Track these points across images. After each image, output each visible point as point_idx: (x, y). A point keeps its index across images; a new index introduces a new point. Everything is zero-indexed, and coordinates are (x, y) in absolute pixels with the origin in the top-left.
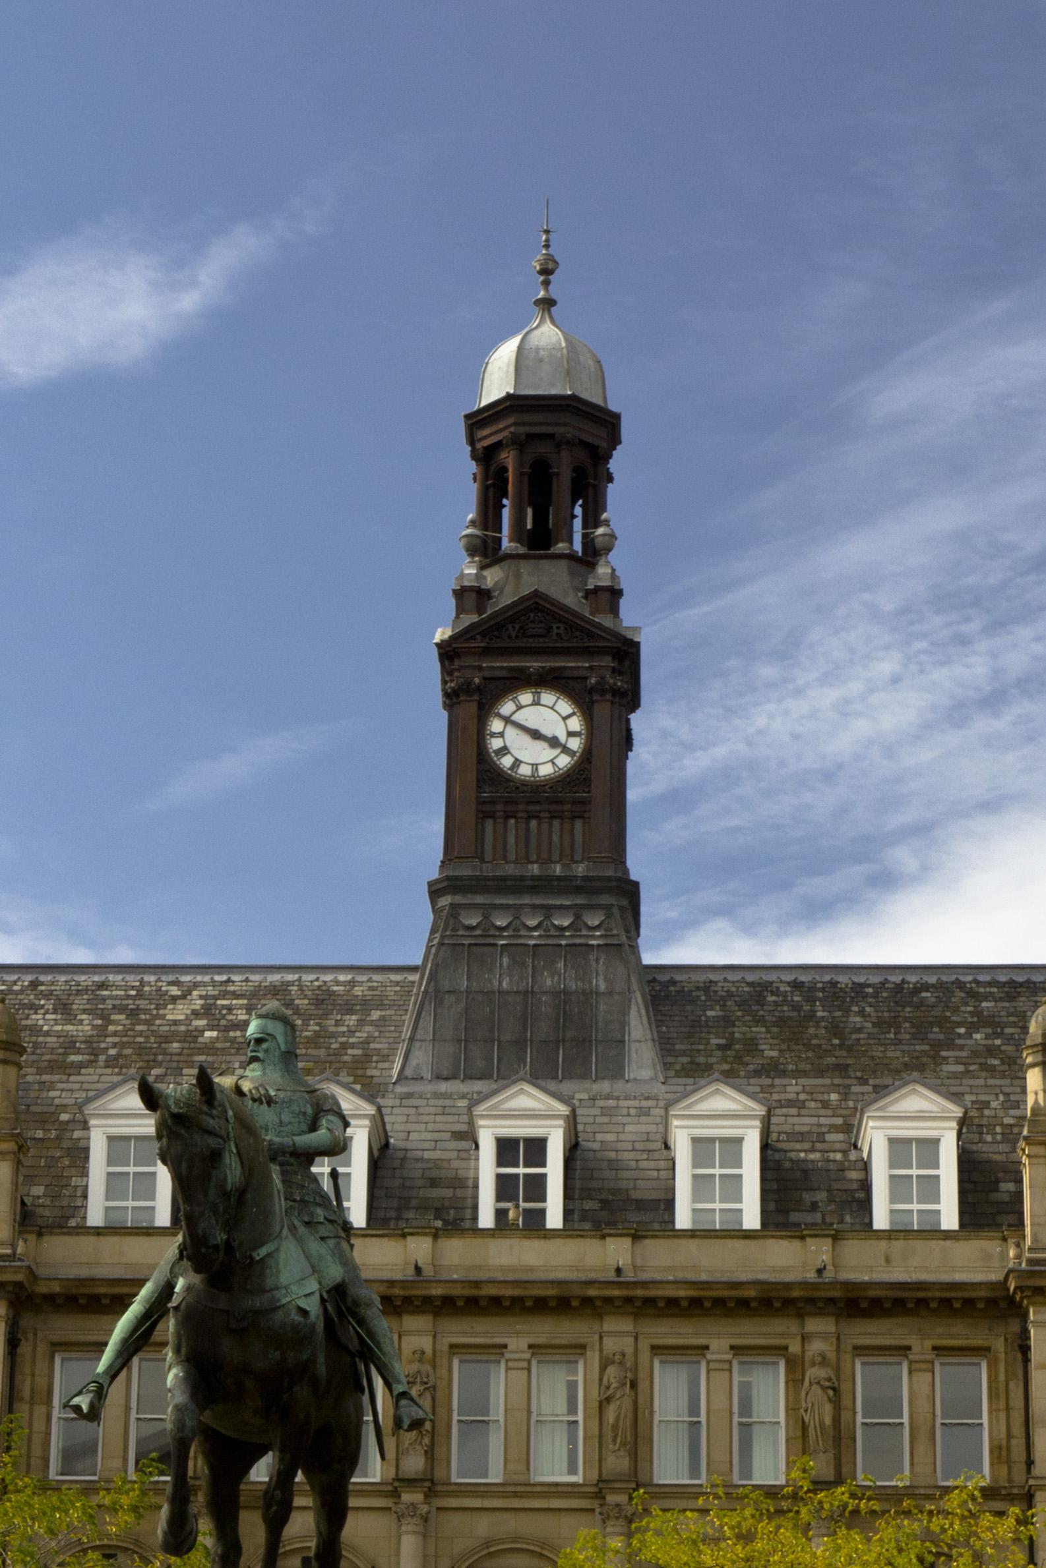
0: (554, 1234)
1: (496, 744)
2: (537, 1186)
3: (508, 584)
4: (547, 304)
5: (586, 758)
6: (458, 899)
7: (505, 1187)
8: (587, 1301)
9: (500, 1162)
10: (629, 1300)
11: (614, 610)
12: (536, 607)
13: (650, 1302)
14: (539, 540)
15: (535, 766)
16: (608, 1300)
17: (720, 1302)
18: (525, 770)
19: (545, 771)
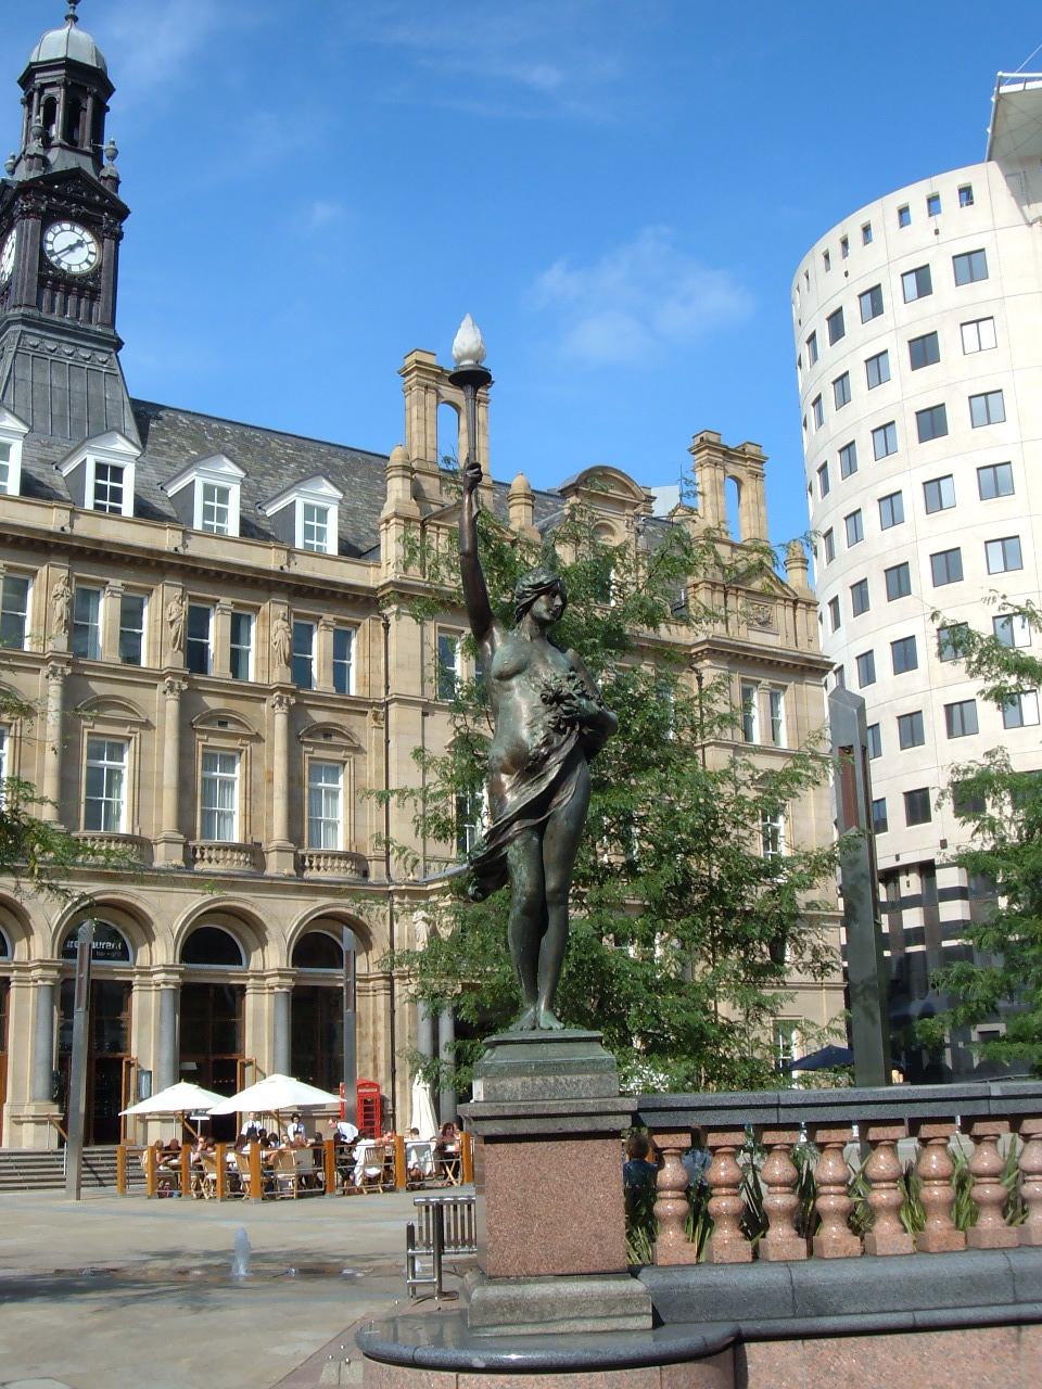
0: (127, 521)
1: (49, 247)
2: (117, 495)
3: (60, 160)
4: (75, 19)
5: (99, 268)
6: (24, 328)
7: (100, 492)
8: (159, 564)
9: (97, 477)
10: (182, 567)
11: (117, 191)
12: (75, 174)
13: (195, 570)
14: (71, 142)
15: (70, 265)
16: (172, 565)
17: (231, 577)
18: (64, 266)
19: (75, 269)
